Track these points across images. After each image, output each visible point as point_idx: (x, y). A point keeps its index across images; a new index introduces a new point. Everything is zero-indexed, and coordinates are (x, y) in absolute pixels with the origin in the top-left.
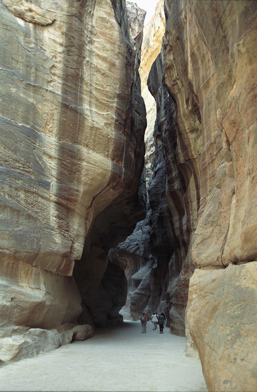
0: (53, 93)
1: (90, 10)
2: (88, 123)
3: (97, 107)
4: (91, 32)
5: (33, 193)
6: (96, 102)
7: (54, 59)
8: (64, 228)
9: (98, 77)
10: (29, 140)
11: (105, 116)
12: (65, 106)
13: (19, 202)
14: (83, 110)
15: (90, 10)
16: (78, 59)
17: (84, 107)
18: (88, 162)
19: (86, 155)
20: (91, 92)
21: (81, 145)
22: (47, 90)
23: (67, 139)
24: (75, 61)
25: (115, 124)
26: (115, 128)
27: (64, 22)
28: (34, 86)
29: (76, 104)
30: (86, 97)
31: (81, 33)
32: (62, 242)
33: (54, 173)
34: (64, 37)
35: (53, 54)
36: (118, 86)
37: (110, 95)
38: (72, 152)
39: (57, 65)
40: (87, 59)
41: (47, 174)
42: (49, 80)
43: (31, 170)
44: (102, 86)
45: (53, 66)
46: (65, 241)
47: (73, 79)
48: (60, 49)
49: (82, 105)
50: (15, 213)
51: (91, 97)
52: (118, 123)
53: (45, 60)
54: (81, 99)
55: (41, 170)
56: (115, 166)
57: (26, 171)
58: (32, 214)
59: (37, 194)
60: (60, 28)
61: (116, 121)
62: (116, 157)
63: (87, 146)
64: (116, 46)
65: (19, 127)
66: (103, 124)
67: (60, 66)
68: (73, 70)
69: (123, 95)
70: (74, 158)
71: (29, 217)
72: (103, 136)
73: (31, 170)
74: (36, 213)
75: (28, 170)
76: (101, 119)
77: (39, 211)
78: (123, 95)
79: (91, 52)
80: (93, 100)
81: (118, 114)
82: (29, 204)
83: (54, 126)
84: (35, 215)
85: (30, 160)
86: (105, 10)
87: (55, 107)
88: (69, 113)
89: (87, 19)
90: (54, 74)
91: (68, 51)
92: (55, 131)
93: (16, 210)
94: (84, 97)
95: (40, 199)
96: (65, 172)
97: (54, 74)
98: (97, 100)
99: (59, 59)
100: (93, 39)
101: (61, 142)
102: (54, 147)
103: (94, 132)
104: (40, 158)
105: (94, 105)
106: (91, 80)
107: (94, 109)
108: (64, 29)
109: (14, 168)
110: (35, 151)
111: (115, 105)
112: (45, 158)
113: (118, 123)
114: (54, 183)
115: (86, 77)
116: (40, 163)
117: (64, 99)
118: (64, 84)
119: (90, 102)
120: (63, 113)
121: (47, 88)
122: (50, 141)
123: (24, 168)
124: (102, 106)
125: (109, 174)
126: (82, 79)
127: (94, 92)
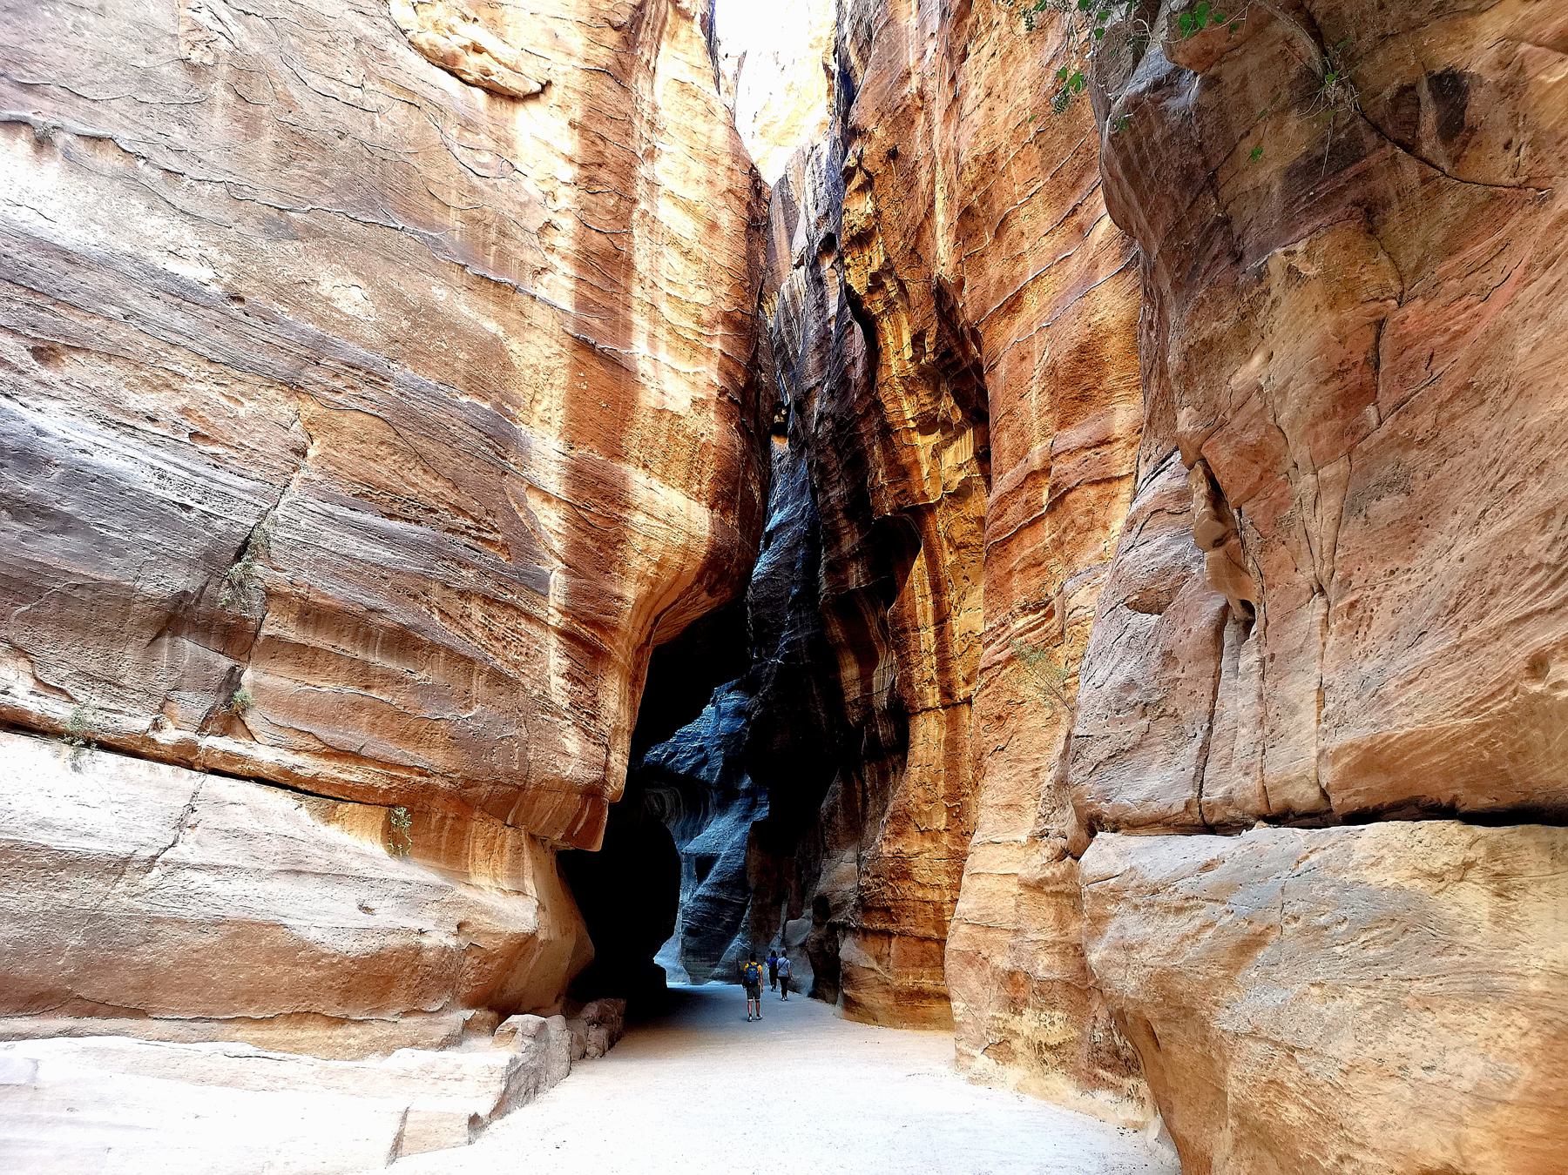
1: (647, 56)
2: (648, 399)
4: (652, 124)
5: (507, 605)
6: (667, 338)
7: (549, 202)
9: (672, 261)
10: (489, 445)
15: (647, 56)
16: (616, 206)
17: (635, 349)
22: (534, 297)
23: (592, 445)
25: (718, 402)
28: (497, 284)
29: (615, 340)
30: (639, 320)
31: (625, 124)
34: (577, 138)
36: (724, 289)
39: (556, 219)
40: (643, 205)
41: (540, 549)
42: (539, 266)
43: (500, 537)
45: (548, 224)
47: (607, 267)
48: (570, 172)
49: (629, 345)
50: (461, 666)
51: (655, 322)
54: (628, 327)
55: (523, 542)
57: (484, 540)
58: (506, 669)
59: (516, 609)
64: (720, 170)
67: (568, 224)
69: (739, 316)
70: (612, 501)
71: (497, 678)
73: (500, 537)
75: (490, 537)
77: (523, 658)
78: (739, 316)
79: (652, 184)
80: (661, 332)
82: (497, 639)
84: (513, 673)
85: (494, 507)
86: (689, 58)
87: (556, 348)
88: (596, 367)
89: (641, 84)
90: (551, 249)
91: (589, 183)
92: (558, 417)
93: (464, 658)
95: (524, 625)
97: (551, 249)
98: (672, 331)
100: (658, 145)
102: (554, 467)
103: (665, 425)
104: (521, 502)
106: (654, 270)
108: (577, 114)
109: (453, 531)
110: (505, 479)
111: (717, 345)
115: (641, 263)
116: (521, 515)
117: (580, 325)
119: (653, 336)
120: (578, 366)
121: (533, 292)
122: (546, 450)
123: (479, 530)
126: (629, 266)
127: (665, 307)
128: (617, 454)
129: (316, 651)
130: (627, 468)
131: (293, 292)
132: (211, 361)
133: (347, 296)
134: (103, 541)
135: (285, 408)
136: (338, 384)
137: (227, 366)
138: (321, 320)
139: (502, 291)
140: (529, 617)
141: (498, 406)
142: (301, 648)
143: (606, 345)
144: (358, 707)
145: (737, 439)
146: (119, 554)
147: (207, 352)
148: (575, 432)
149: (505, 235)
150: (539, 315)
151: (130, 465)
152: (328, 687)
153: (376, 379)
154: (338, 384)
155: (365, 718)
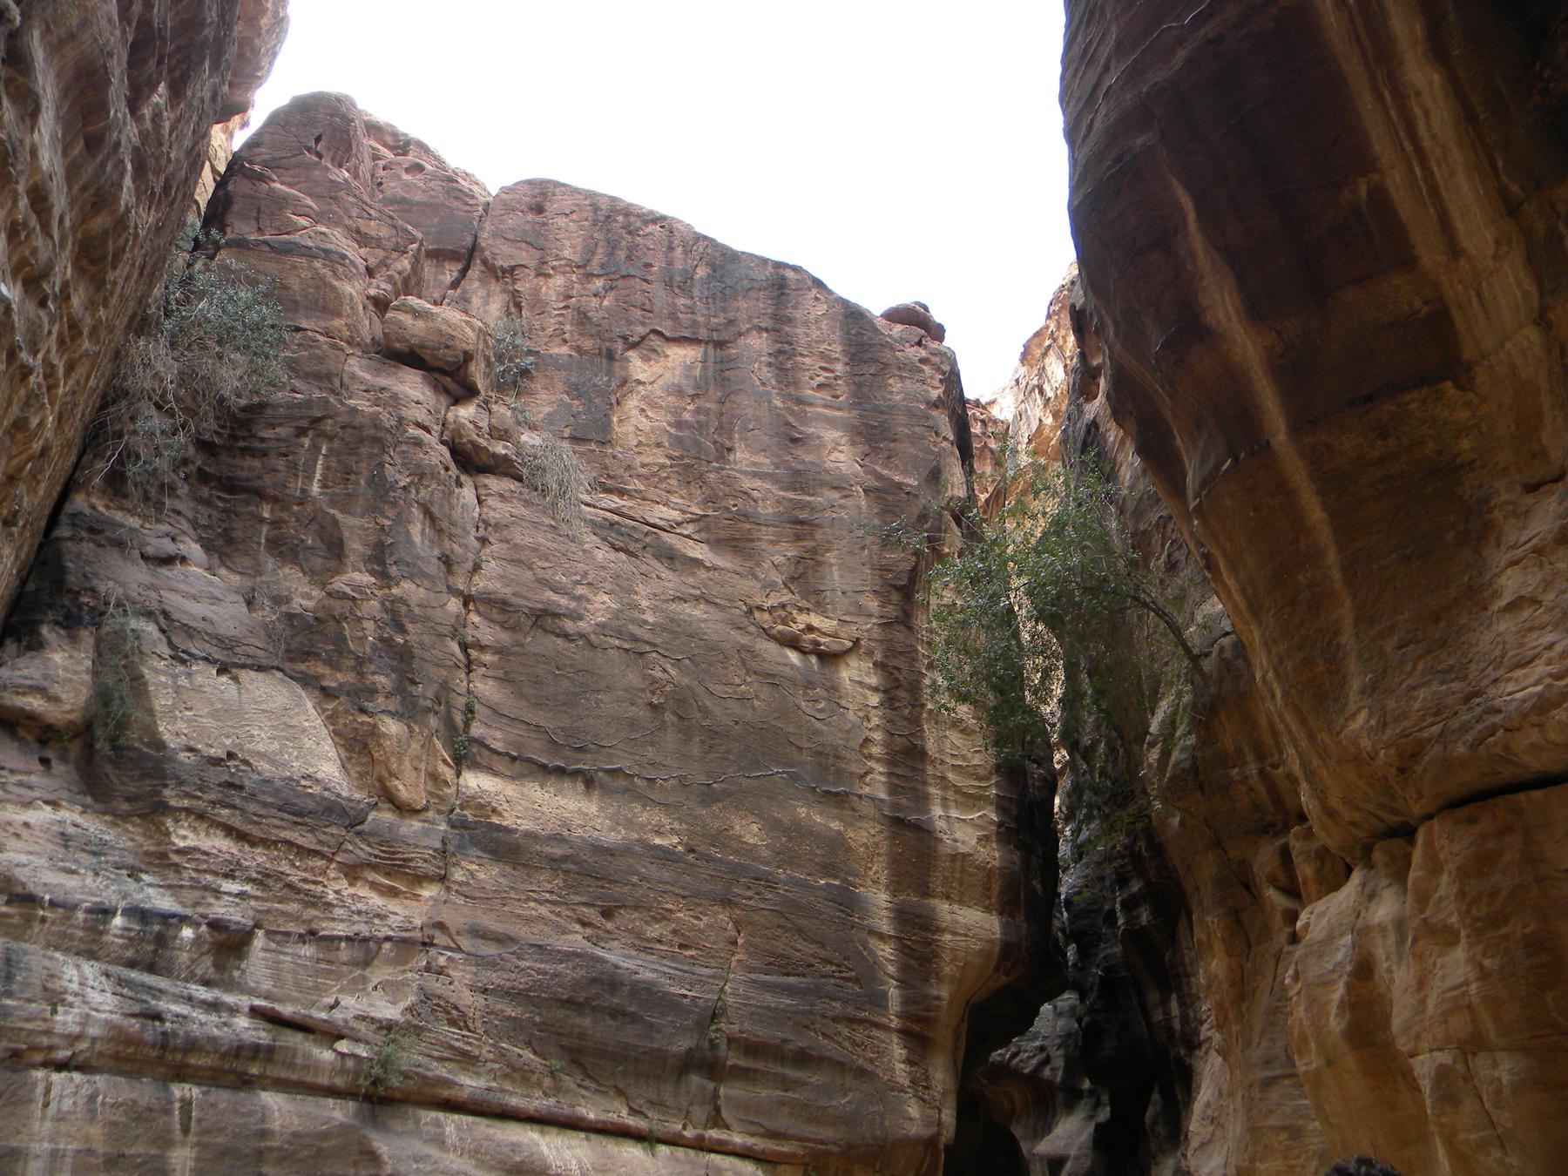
0: (873, 799)
3: (958, 805)
8: (921, 1084)
12: (898, 823)
13: (840, 1044)
14: (931, 821)
18: (954, 933)
19: (948, 917)
20: (944, 778)
21: (934, 897)
22: (860, 796)
26: (999, 841)
28: (837, 794)
31: (910, 654)
32: (922, 1114)
33: (891, 969)
35: (861, 714)
37: (982, 772)
38: (919, 917)
44: (964, 758)
46: (928, 1111)
47: (908, 758)
48: (874, 699)
49: (928, 811)
51: (945, 788)
53: (849, 732)
56: (1004, 926)
57: (844, 979)
60: (870, 653)
61: (1000, 825)
62: (1006, 906)
63: (948, 897)
65: (821, 888)
67: (877, 736)
74: (872, 1061)
76: (969, 830)
80: (950, 794)
83: (879, 869)
84: (869, 1067)
87: (878, 828)
90: (870, 757)
91: (890, 701)
94: (933, 790)
95: (876, 1033)
96: (913, 962)
97: (870, 757)
98: (958, 790)
99: (875, 721)
101: (896, 900)
103: (958, 863)
105: (953, 804)
106: (941, 751)
107: (954, 813)
108: (878, 656)
112: (873, 942)
114: (893, 993)
115: (931, 746)
118: (890, 774)
119: (944, 799)
120: (893, 837)
122: (879, 900)
124: (971, 800)
125: (997, 950)
127: (950, 776)
128: (927, 894)
129: (756, 1071)
130: (935, 902)
131: (721, 838)
132: (684, 897)
133: (750, 832)
134: (651, 1025)
135: (723, 917)
136: (749, 893)
137: (692, 898)
138: (736, 852)
139: (838, 800)
140: (878, 1026)
141: (845, 881)
142: (748, 1070)
143: (912, 817)
144: (782, 1103)
145: (1016, 857)
146: (659, 1031)
147: (681, 891)
148: (896, 885)
149: (838, 757)
150: (867, 808)
151: (654, 975)
152: (766, 1093)
153: (770, 883)
154: (749, 893)
155: (786, 1110)
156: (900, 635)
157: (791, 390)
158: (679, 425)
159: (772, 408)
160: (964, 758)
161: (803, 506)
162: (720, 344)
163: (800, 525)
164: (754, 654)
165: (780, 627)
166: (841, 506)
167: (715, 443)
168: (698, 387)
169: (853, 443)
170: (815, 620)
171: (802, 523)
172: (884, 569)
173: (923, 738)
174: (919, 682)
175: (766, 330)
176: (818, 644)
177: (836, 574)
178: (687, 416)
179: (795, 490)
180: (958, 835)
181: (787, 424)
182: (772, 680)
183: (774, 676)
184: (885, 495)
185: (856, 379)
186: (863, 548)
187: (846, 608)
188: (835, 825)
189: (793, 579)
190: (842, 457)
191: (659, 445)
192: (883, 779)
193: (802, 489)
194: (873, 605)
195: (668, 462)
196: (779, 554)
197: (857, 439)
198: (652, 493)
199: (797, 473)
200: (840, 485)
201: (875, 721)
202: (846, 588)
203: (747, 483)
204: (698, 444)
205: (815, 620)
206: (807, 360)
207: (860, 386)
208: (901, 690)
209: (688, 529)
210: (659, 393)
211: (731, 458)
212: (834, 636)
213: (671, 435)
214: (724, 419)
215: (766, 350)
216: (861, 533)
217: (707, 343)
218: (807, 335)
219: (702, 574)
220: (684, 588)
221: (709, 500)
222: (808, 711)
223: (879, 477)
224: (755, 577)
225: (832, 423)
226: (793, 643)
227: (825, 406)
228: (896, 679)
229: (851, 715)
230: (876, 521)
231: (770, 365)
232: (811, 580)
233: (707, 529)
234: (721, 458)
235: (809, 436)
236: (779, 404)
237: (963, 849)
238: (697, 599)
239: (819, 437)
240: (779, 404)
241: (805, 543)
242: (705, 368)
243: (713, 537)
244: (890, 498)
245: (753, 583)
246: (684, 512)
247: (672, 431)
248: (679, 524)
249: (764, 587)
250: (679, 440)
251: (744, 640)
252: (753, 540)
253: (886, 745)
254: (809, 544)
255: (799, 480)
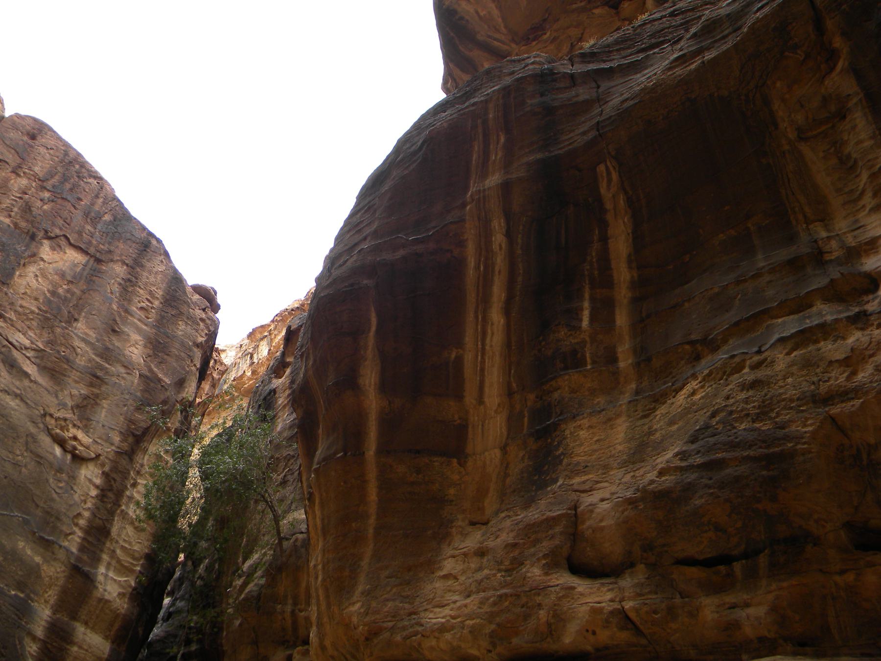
11: (124, 584)
14: (96, 574)
16: (111, 508)
20: (114, 551)
24: (107, 509)
27: (110, 460)
30: (105, 557)
31: (125, 475)
35: (83, 498)
37: (137, 555)
40: (123, 507)
44: (130, 543)
47: (98, 533)
48: (94, 492)
49: (96, 568)
51: (112, 557)
52: (135, 592)
53: (71, 506)
56: (112, 650)
61: (134, 589)
66: (115, 594)
67: (86, 514)
68: (101, 522)
72: (111, 611)
76: (116, 586)
79: (131, 498)
80: (114, 562)
81: (139, 583)
90: (76, 525)
91: (102, 496)
97: (76, 525)
98: (119, 561)
99: (89, 505)
103: (101, 604)
105: (112, 568)
106: (119, 535)
107: (111, 574)
113: (135, 592)
115: (114, 531)
118: (84, 539)
119: (109, 564)
127: (118, 552)
156: (124, 462)
157: (125, 303)
158: (54, 293)
159: (110, 308)
160: (130, 543)
161: (102, 368)
162: (99, 261)
163: (96, 378)
164: (35, 441)
165: (58, 431)
166: (123, 378)
167: (69, 312)
168: (74, 277)
169: (145, 347)
170: (80, 435)
171: (98, 377)
172: (131, 421)
173: (112, 524)
174: (123, 491)
175: (127, 265)
176: (75, 448)
177: (103, 413)
178: (60, 291)
179: (102, 358)
180: (109, 588)
181: (115, 320)
182: (39, 459)
183: (41, 458)
184: (149, 381)
185: (163, 313)
186: (125, 406)
187: (99, 436)
188: (38, 559)
189: (78, 406)
190: (136, 351)
191: (36, 299)
192: (79, 540)
193: (106, 359)
194: (117, 439)
195: (37, 311)
196: (77, 389)
197: (148, 345)
198: (19, 325)
199: (107, 349)
200: (128, 367)
201: (89, 505)
202: (106, 423)
203: (77, 343)
204: (59, 309)
205: (80, 435)
206: (141, 291)
207: (163, 317)
208: (112, 492)
209: (30, 354)
210: (51, 271)
211: (74, 325)
212: (87, 448)
213: (46, 297)
214: (81, 302)
215: (122, 275)
216: (127, 397)
217: (91, 256)
218: (148, 278)
219: (26, 383)
220: (11, 386)
221: (51, 343)
222: (53, 485)
223: (151, 370)
224: (57, 397)
225: (139, 330)
226: (61, 442)
227: (139, 320)
228: (111, 486)
229: (76, 497)
230: (139, 394)
231: (120, 284)
232: (88, 411)
233: (42, 358)
234: (69, 322)
235: (123, 332)
236: (115, 307)
237: (107, 597)
238: (16, 396)
239: (128, 335)
240: (115, 307)
241: (93, 390)
242: (83, 269)
243: (43, 364)
244: (152, 384)
245: (54, 400)
246: (32, 343)
247: (48, 295)
248: (26, 348)
249: (59, 404)
250: (50, 301)
251: (33, 430)
252: (65, 376)
253: (89, 521)
254: (96, 391)
255: (107, 354)
